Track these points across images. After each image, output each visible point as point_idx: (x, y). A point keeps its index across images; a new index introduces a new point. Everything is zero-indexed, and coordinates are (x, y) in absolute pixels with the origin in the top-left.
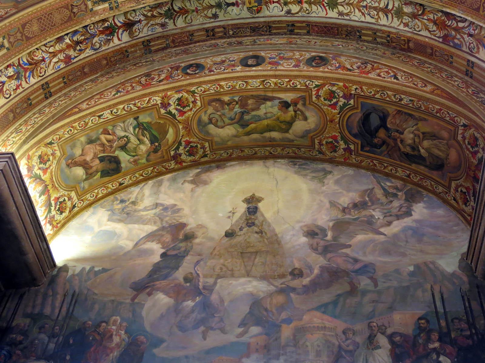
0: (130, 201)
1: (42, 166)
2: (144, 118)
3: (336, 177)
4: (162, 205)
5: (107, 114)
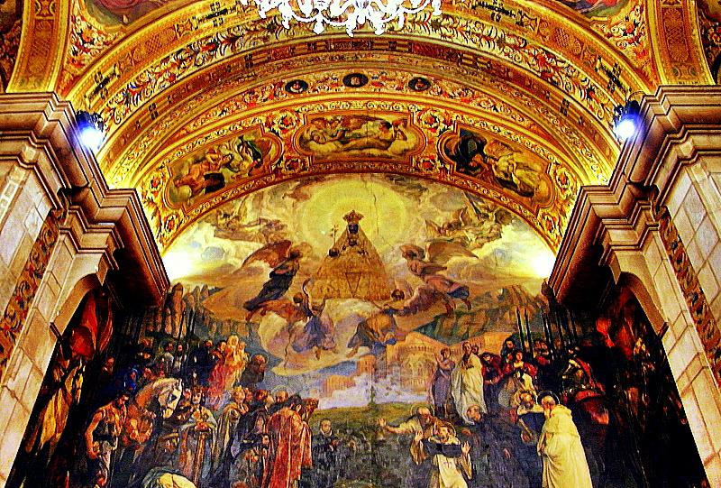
0: (234, 215)
1: (154, 189)
2: (248, 138)
3: (431, 196)
4: (266, 221)
5: (214, 135)
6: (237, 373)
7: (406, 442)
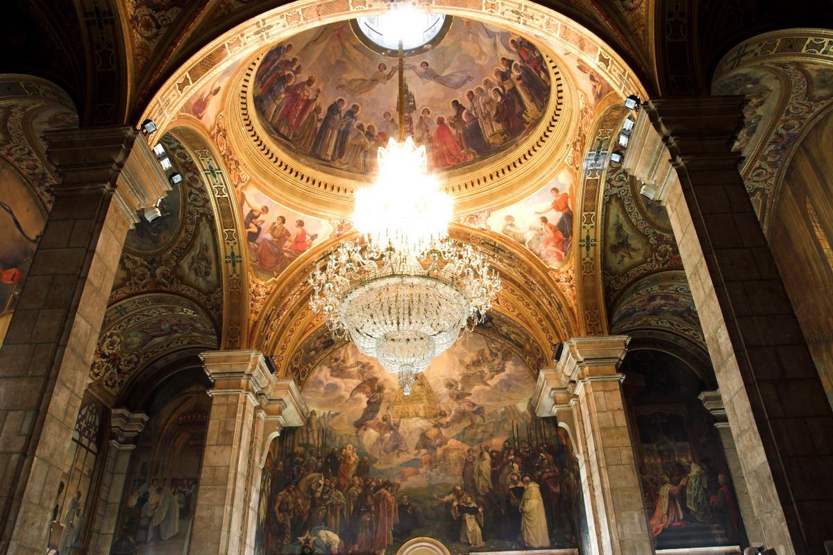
4: (361, 363)
6: (354, 468)
7: (448, 505)
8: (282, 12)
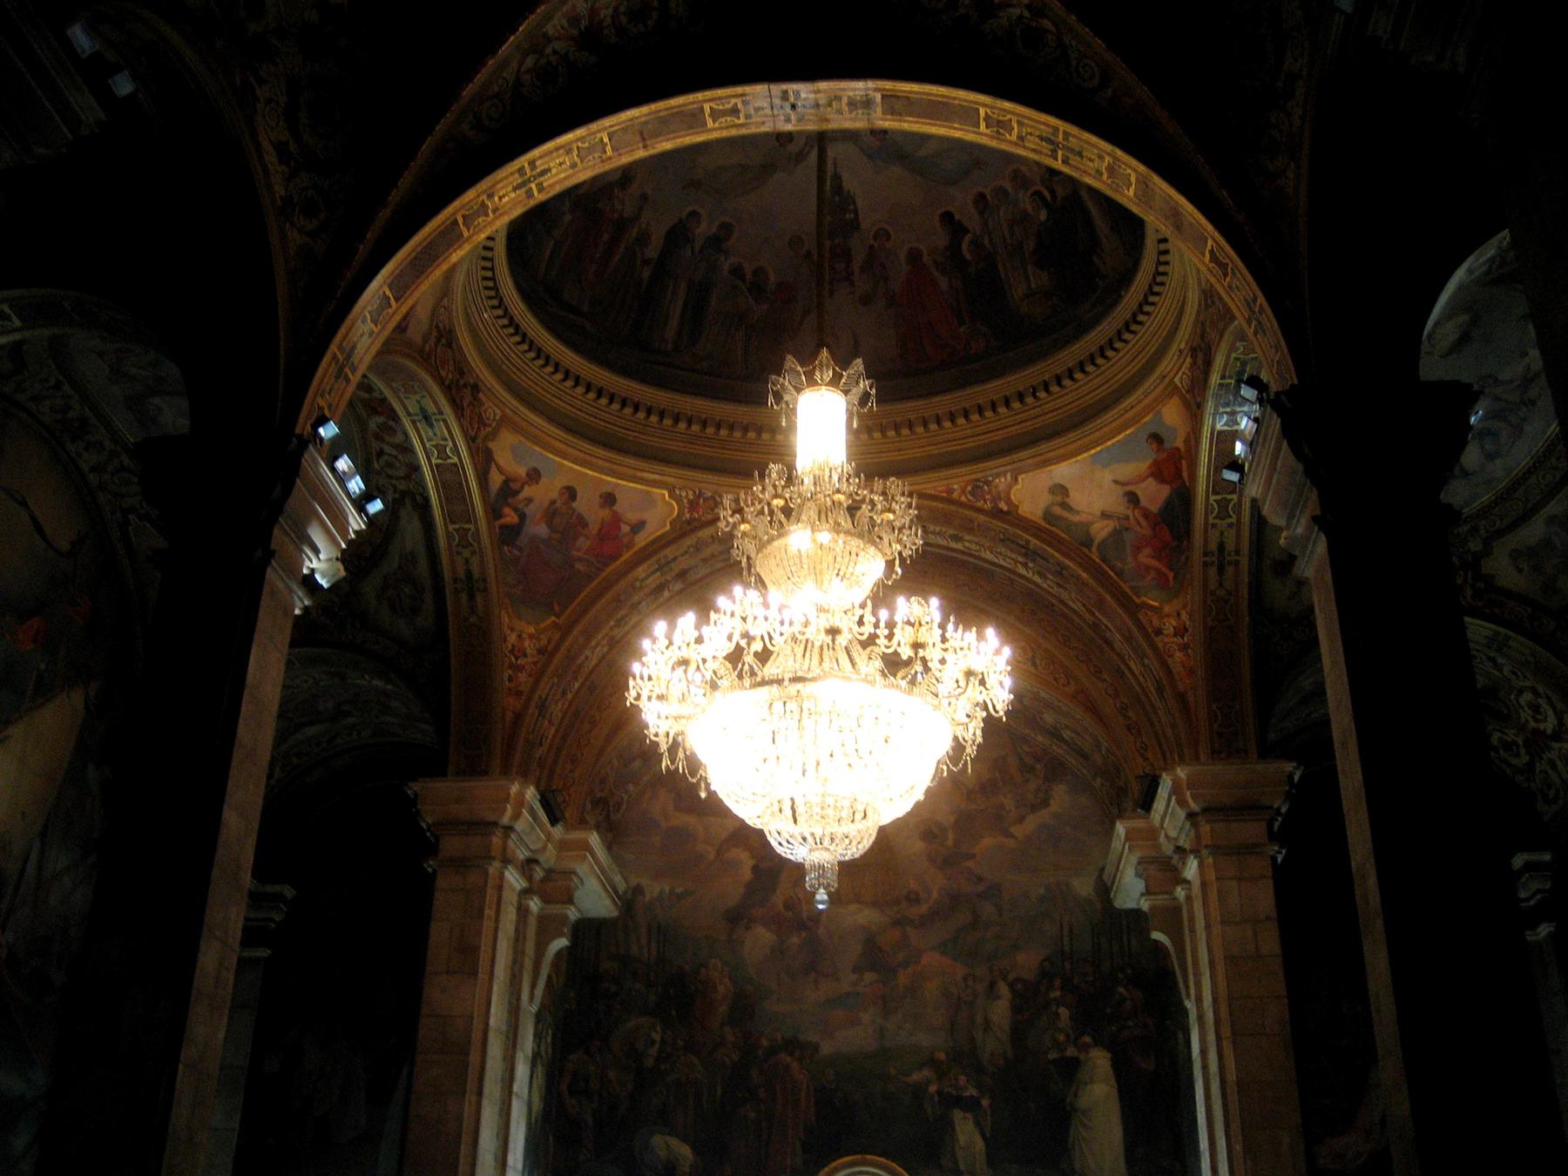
6: (723, 1009)
7: (919, 1091)
8: (570, 143)
